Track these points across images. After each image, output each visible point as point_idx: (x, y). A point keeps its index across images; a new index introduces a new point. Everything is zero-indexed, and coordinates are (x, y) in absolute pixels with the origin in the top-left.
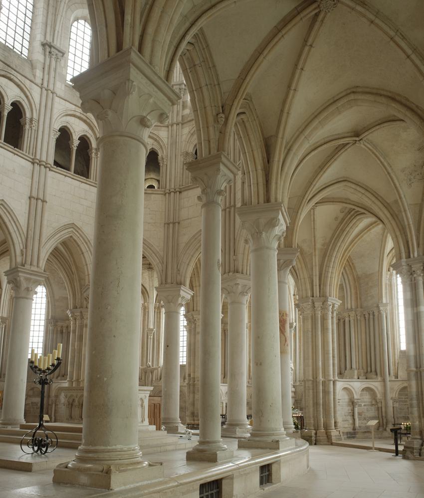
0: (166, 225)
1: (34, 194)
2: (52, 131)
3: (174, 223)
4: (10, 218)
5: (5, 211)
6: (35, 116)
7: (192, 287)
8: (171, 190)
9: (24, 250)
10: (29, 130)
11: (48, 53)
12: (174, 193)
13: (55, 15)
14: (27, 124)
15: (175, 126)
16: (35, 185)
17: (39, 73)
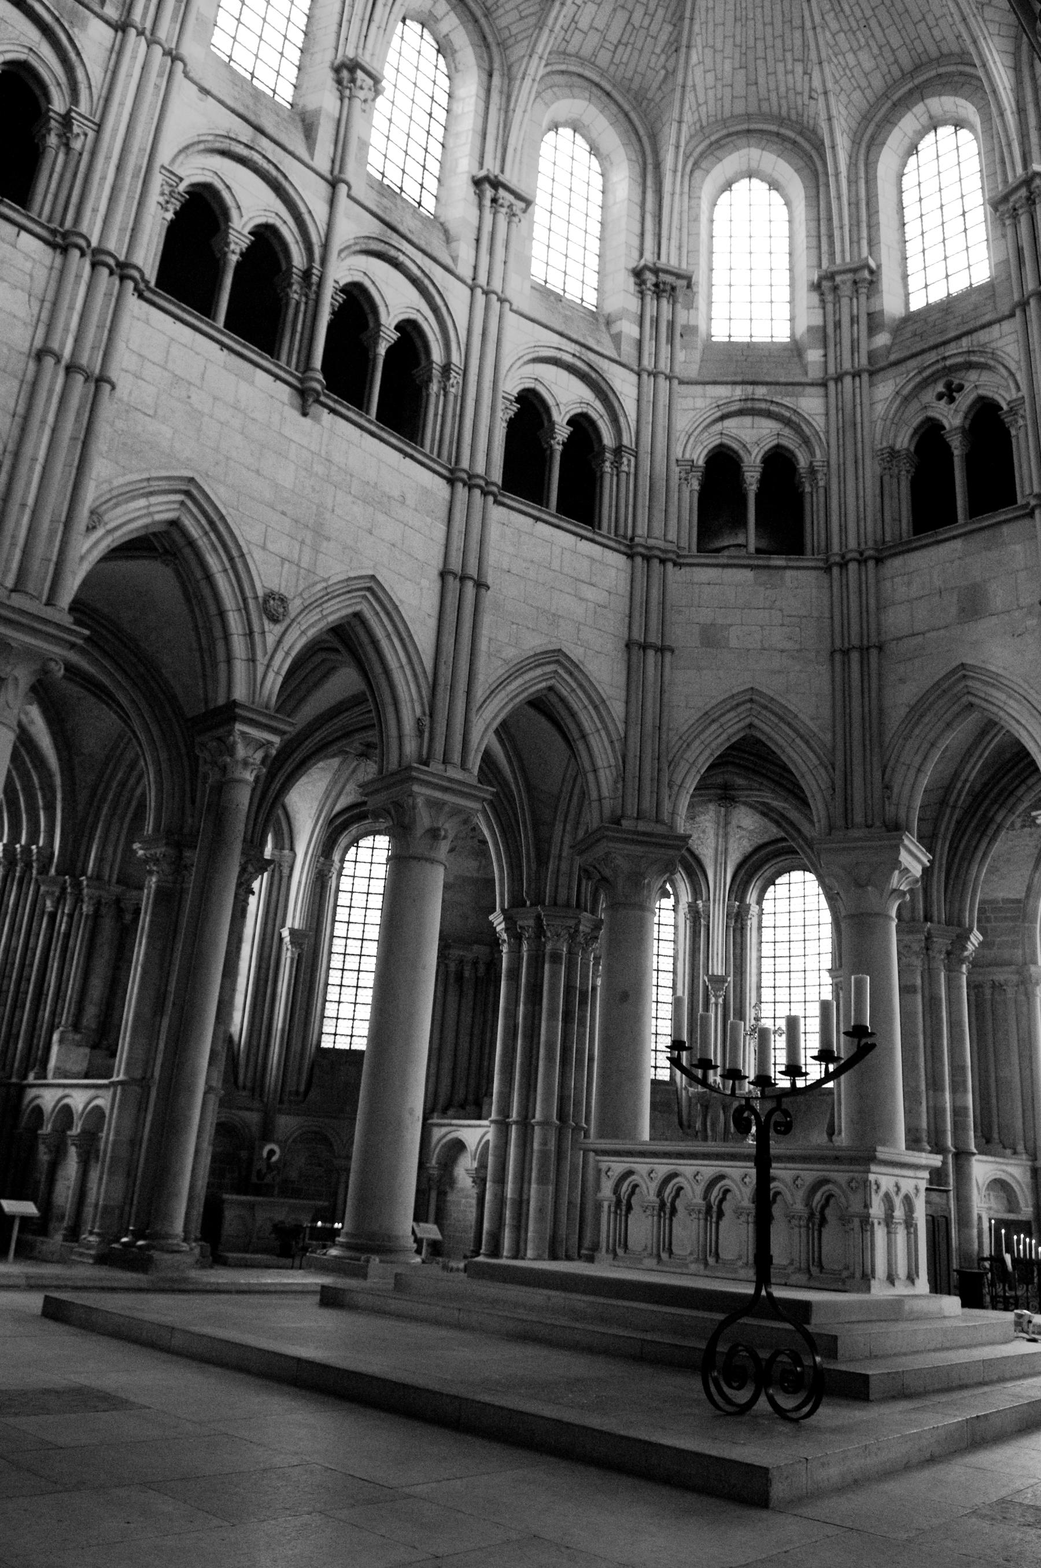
0: (838, 657)
1: (455, 565)
2: (500, 401)
3: (864, 650)
4: (390, 628)
5: (378, 608)
6: (456, 359)
7: (928, 841)
8: (849, 556)
9: (427, 721)
10: (438, 396)
11: (487, 202)
12: (859, 562)
13: (507, 112)
14: (435, 381)
15: (848, 380)
16: (457, 542)
17: (465, 251)
